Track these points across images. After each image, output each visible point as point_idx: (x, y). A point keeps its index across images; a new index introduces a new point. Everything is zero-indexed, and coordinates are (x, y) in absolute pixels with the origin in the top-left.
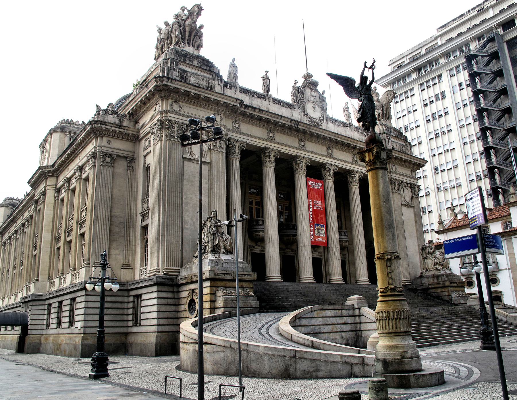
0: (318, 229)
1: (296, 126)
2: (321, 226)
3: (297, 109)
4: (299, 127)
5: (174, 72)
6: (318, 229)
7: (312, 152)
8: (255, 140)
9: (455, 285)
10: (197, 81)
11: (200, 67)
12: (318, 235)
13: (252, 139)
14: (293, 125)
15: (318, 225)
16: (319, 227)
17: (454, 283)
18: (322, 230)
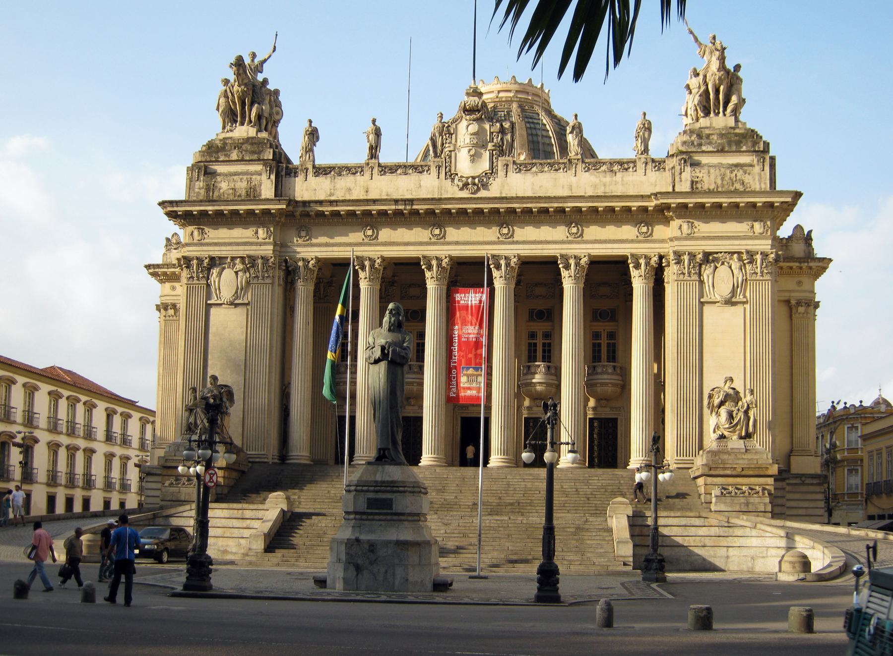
0: (468, 376)
1: (408, 207)
2: (476, 369)
3: (433, 170)
4: (415, 207)
5: (197, 183)
6: (468, 376)
7: (457, 243)
8: (335, 249)
9: (728, 472)
10: (232, 185)
11: (242, 160)
12: (466, 385)
13: (330, 249)
14: (400, 207)
15: (468, 369)
16: (471, 371)
17: (725, 468)
18: (477, 376)
